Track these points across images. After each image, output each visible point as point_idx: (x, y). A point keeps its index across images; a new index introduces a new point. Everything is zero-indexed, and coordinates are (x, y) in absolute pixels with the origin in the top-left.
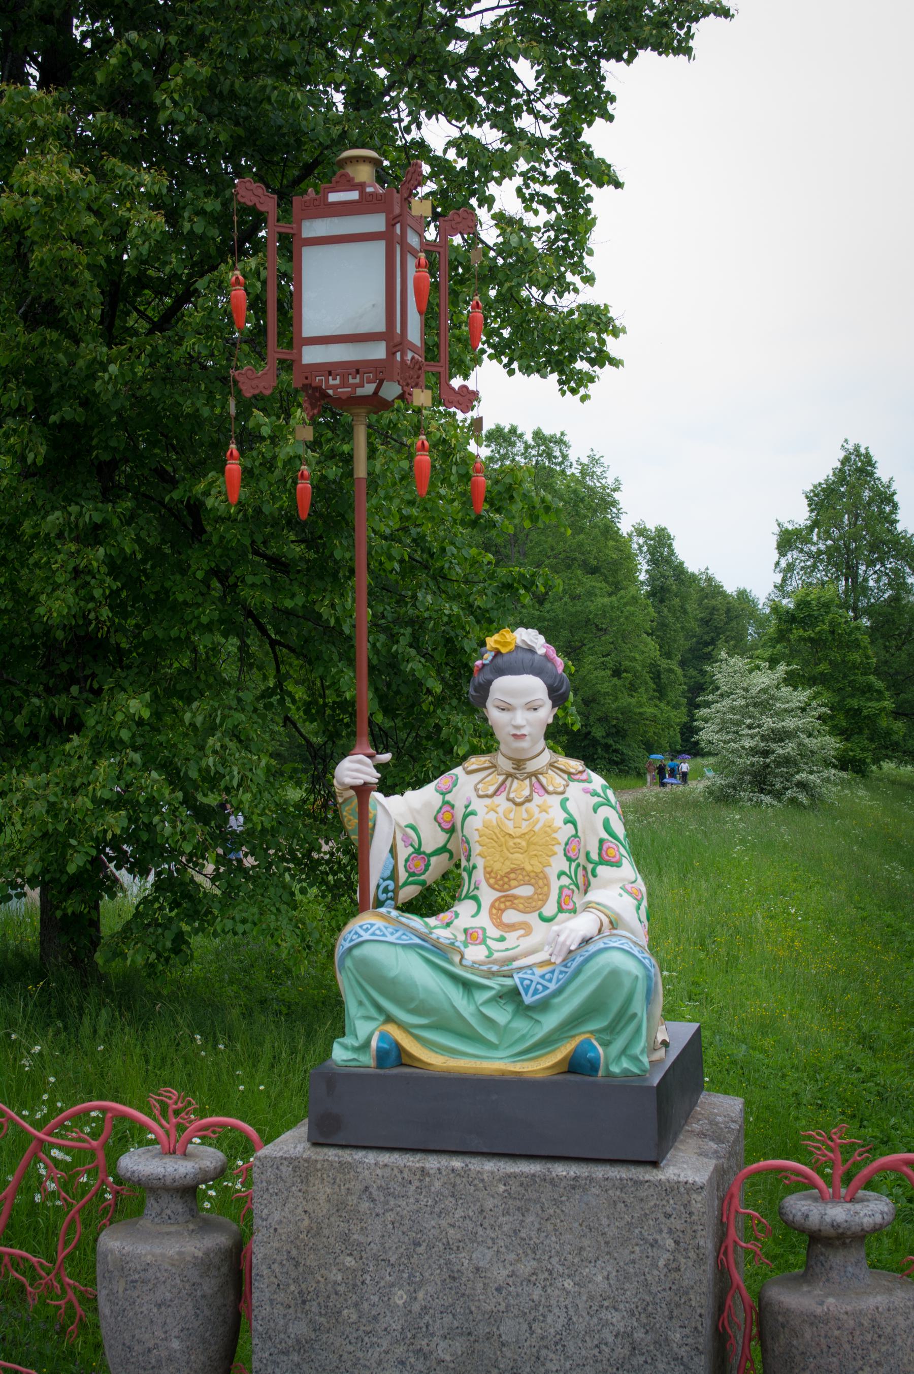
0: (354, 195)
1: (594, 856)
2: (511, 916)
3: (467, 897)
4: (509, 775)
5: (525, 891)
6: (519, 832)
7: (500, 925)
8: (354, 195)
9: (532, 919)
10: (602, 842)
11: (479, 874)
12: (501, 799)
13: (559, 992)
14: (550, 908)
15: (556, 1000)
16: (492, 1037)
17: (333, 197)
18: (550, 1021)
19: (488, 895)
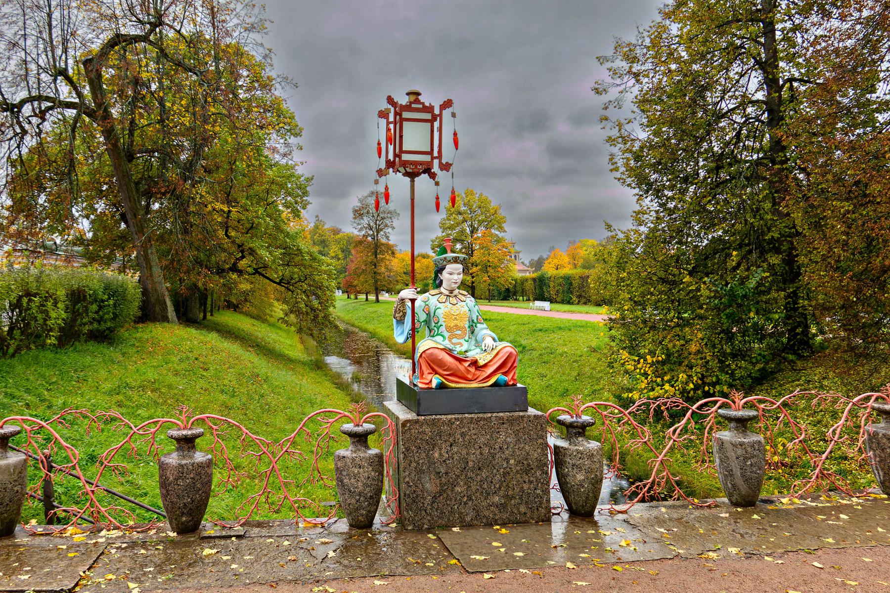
0: (421, 106)
1: (475, 321)
2: (454, 340)
3: (437, 335)
4: (447, 296)
5: (459, 332)
6: (455, 314)
7: (453, 344)
8: (421, 106)
9: (462, 341)
10: (477, 316)
11: (443, 329)
12: (448, 303)
13: (491, 361)
14: (467, 338)
15: (491, 363)
16: (470, 376)
17: (413, 106)
18: (490, 370)
19: (446, 334)
